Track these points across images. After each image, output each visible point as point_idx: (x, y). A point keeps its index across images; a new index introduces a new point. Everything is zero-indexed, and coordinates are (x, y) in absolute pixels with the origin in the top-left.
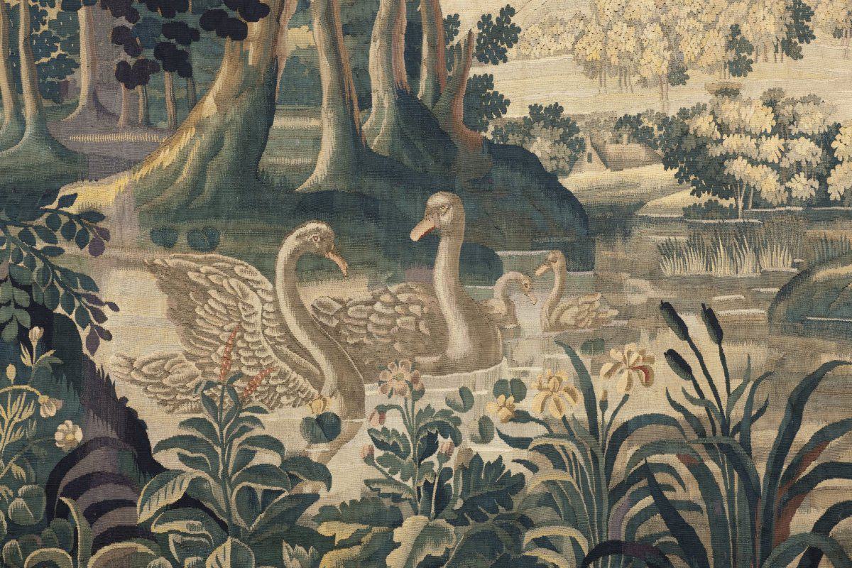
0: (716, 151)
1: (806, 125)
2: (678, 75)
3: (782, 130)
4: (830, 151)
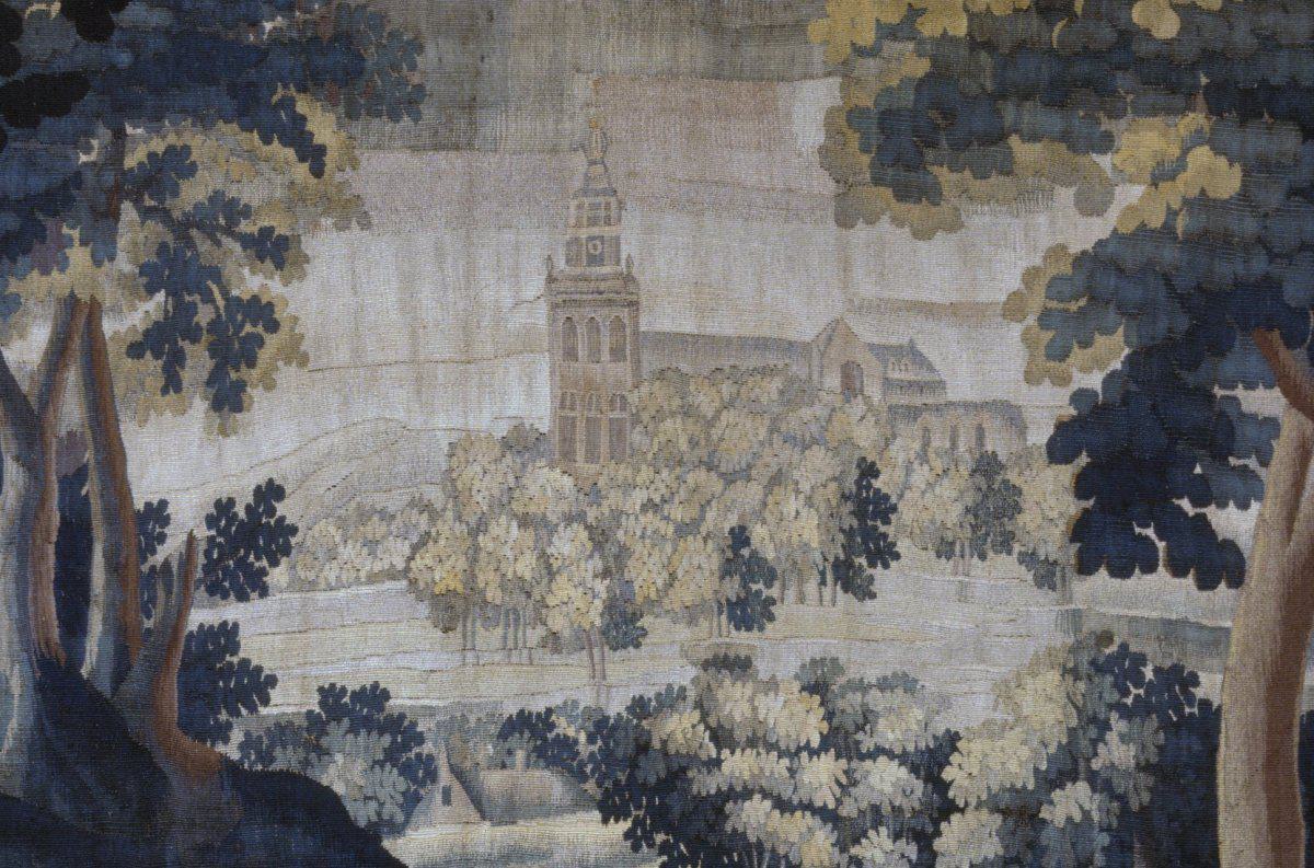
0: (707, 784)
1: (888, 733)
2: (623, 626)
3: (842, 740)
4: (942, 787)
